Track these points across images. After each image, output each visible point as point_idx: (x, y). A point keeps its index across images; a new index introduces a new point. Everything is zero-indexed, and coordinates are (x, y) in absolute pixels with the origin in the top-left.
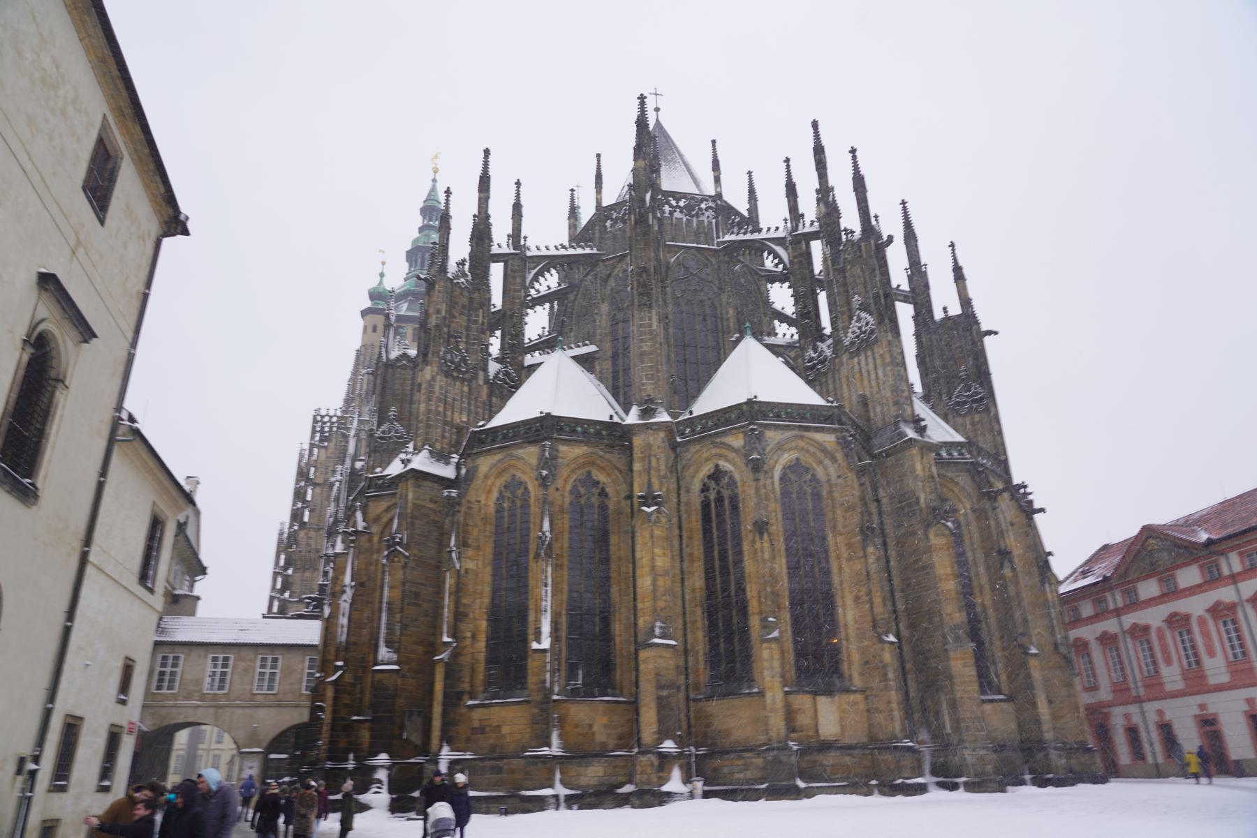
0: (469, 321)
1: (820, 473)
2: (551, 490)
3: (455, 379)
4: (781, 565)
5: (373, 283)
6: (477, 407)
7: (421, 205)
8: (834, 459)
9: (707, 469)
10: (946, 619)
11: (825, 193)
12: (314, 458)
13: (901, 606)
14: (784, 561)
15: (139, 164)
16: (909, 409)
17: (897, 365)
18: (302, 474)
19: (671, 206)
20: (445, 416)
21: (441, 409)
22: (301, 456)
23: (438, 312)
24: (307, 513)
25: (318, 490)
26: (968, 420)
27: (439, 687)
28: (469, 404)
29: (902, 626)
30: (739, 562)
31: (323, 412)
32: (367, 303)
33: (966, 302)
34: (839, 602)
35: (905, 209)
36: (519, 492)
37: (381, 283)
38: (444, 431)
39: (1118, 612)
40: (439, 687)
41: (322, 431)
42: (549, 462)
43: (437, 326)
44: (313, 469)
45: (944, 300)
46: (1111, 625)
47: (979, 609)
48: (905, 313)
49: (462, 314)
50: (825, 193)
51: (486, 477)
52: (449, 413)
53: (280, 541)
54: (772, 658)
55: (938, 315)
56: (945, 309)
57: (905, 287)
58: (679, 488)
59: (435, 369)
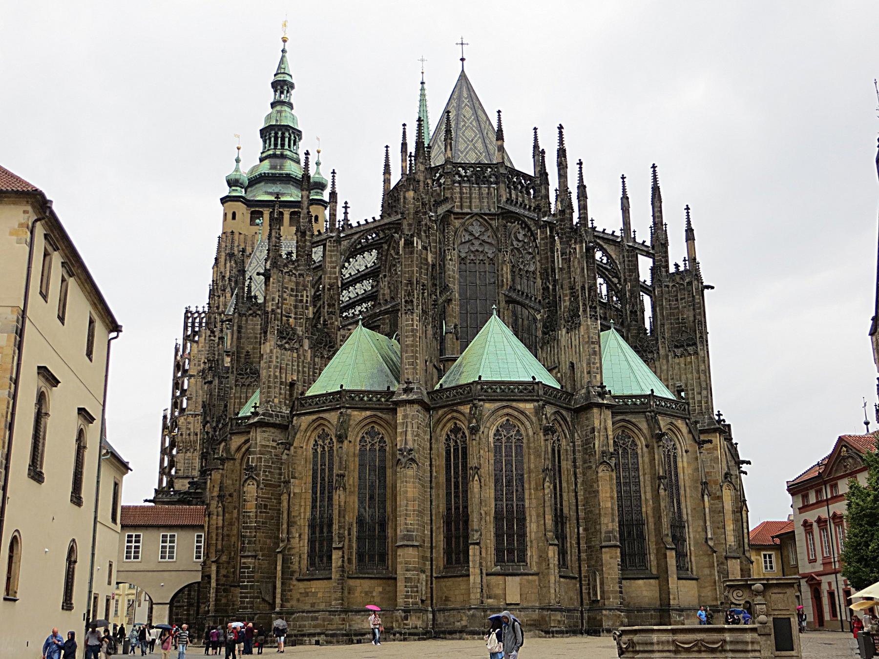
0: (296, 301)
1: (523, 431)
2: (346, 442)
3: (286, 349)
4: (490, 493)
5: (229, 170)
6: (304, 367)
7: (272, 79)
8: (532, 423)
9: (450, 425)
10: (604, 529)
11: (563, 191)
12: (188, 351)
13: (582, 514)
14: (493, 491)
15: (104, 321)
16: (598, 376)
17: (593, 343)
18: (178, 366)
19: (460, 176)
20: (281, 377)
21: (278, 374)
22: (177, 350)
23: (273, 300)
24: (185, 401)
25: (192, 380)
26: (682, 360)
27: (279, 568)
28: (298, 366)
29: (581, 529)
30: (465, 492)
31: (193, 310)
32: (226, 191)
33: (692, 260)
34: (528, 518)
35: (654, 171)
36: (327, 442)
37: (237, 170)
38: (281, 389)
39: (827, 502)
40: (279, 568)
41: (193, 326)
42: (344, 425)
43: (273, 310)
44: (187, 361)
45: (677, 255)
46: (822, 512)
47: (644, 515)
48: (645, 265)
49: (291, 295)
50: (563, 191)
51: (306, 431)
52: (283, 376)
53: (165, 427)
54: (474, 555)
55: (672, 269)
56: (677, 266)
57: (648, 243)
58: (431, 439)
59: (272, 343)
